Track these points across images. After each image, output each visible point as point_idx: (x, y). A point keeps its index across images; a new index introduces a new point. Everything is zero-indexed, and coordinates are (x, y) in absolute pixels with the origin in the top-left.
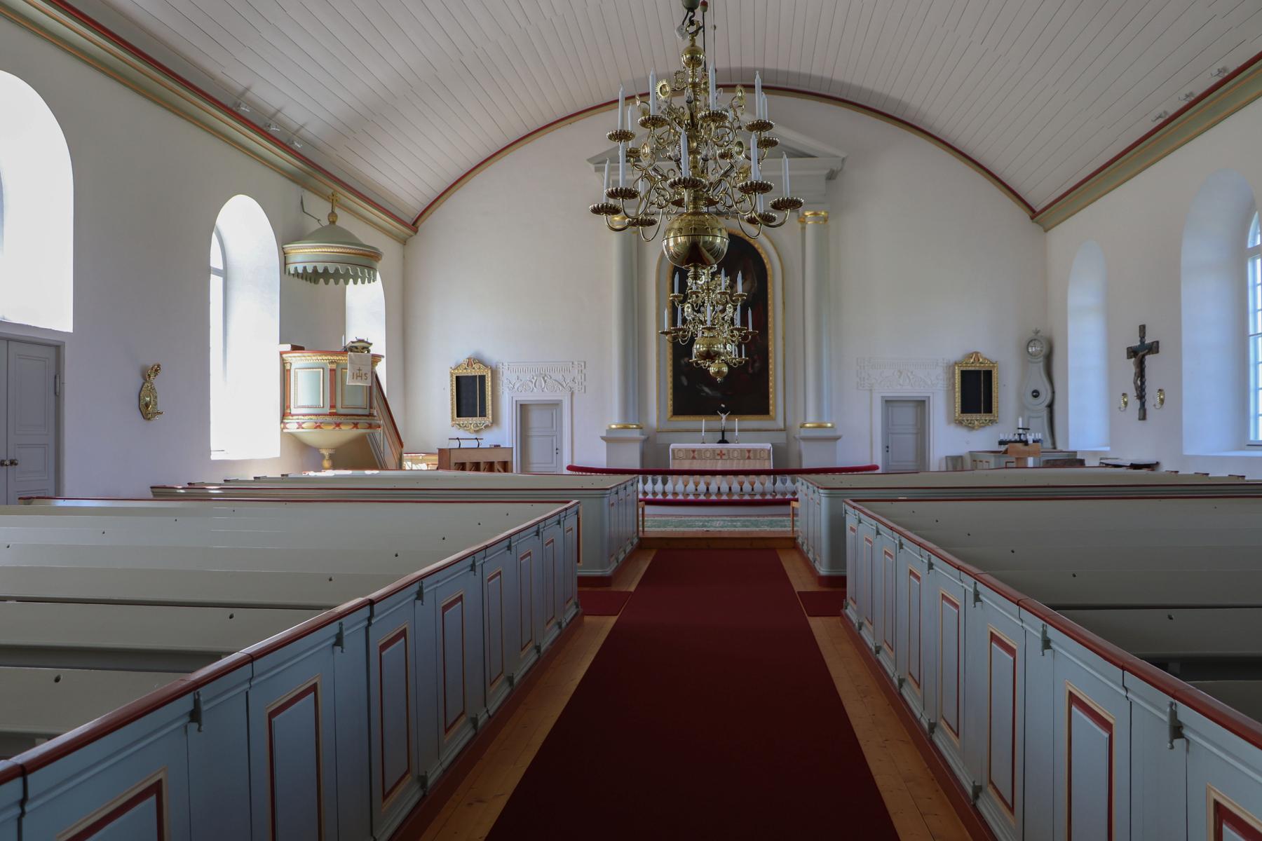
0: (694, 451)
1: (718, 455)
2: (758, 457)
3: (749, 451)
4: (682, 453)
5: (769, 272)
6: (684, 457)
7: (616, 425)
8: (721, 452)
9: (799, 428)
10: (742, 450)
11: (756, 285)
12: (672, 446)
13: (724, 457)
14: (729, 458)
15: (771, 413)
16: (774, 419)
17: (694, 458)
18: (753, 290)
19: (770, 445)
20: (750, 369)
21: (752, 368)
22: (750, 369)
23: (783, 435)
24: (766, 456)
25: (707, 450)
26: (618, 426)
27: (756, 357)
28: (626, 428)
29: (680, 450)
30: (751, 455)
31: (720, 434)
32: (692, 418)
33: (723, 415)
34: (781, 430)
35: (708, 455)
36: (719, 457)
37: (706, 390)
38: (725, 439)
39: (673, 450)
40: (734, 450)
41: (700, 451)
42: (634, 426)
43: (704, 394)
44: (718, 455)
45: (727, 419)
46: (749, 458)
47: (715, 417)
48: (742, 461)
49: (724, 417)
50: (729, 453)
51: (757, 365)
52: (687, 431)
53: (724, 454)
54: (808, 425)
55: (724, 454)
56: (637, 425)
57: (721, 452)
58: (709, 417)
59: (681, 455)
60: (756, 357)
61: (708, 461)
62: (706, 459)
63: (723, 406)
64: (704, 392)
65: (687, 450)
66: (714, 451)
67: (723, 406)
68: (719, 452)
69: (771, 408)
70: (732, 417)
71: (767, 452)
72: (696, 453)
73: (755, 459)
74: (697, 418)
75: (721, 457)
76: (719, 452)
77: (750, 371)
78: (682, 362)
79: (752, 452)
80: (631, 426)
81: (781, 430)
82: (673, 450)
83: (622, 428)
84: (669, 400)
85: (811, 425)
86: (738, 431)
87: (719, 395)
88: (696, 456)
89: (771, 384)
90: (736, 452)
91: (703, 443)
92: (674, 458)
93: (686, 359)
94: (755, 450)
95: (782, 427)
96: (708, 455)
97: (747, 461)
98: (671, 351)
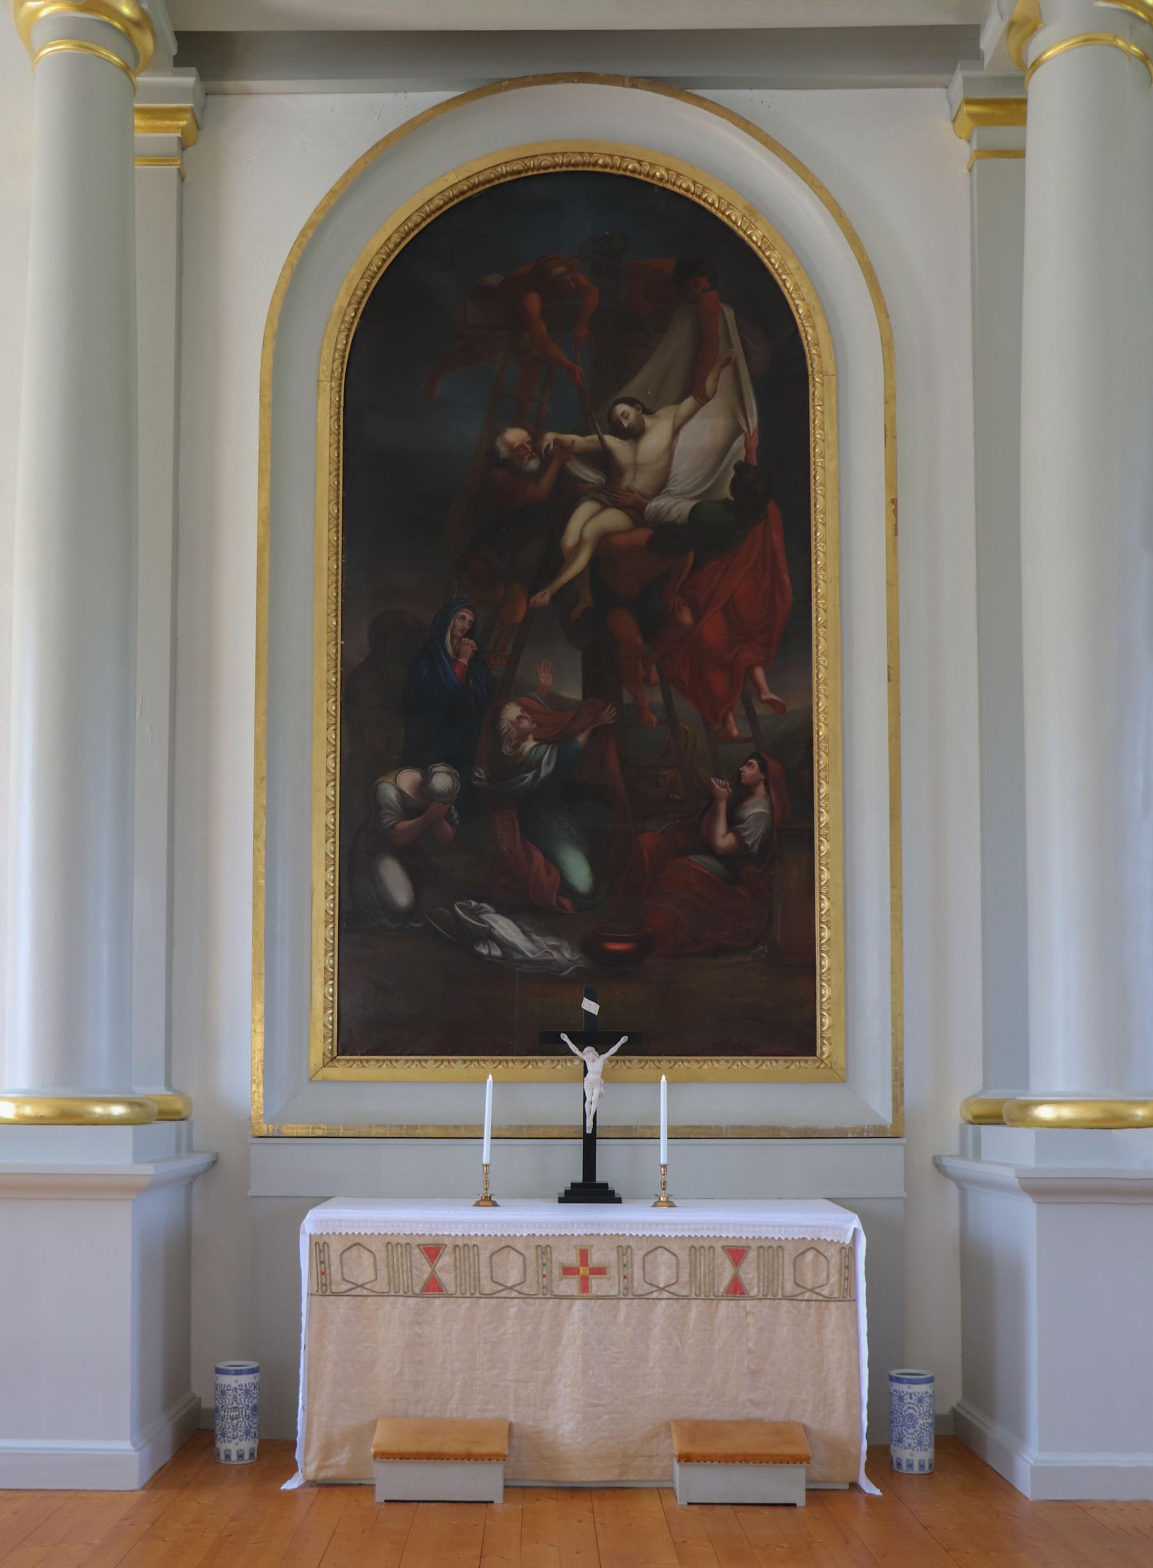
0: (432, 1252)
1: (568, 1271)
2: (789, 1287)
3: (737, 1254)
4: (367, 1259)
5: (819, 359)
6: (382, 1286)
7: (19, 1101)
8: (584, 1255)
9: (955, 1115)
10: (697, 1248)
11: (754, 421)
12: (313, 1223)
13: (597, 1285)
14: (628, 1293)
15: (825, 1049)
16: (839, 1076)
17: (433, 1287)
18: (740, 441)
19: (855, 1223)
20: (721, 826)
21: (733, 823)
22: (721, 826)
23: (888, 1154)
24: (832, 1287)
25: (505, 1246)
26: (28, 1110)
27: (750, 771)
28: (68, 1118)
29: (356, 1244)
30: (749, 1273)
31: (576, 1148)
32: (431, 1068)
33: (589, 1054)
34: (878, 1133)
35: (513, 1276)
36: (570, 1286)
37: (505, 928)
38: (600, 1178)
39: (320, 1246)
40: (657, 1245)
41: (466, 1248)
42: (118, 1110)
43: (497, 952)
44: (568, 1271)
45: (607, 1077)
46: (736, 1289)
47: (545, 1065)
48: (696, 1309)
49: (595, 1061)
50: (625, 1263)
51: (756, 808)
52: (409, 1134)
53: (600, 1271)
54: (1045, 1113)
55: (600, 1271)
56: (130, 1103)
57: (584, 1255)
58: (516, 1066)
59: (363, 1269)
60: (750, 771)
61: (514, 1308)
62: (502, 1292)
63: (590, 1006)
64: (490, 936)
65: (395, 1246)
66: (543, 1249)
67: (590, 1006)
68: (573, 1259)
69: (825, 1022)
70: (634, 1064)
71: (833, 1254)
72: (445, 1260)
73: (770, 1294)
74: (458, 1067)
75: (585, 1287)
76: (573, 1259)
77: (724, 839)
78: (388, 791)
79: (752, 1255)
80: (98, 1110)
81: (878, 1133)
82: (320, 1246)
83: (38, 1121)
84: (319, 979)
85: (1066, 1112)
86: (675, 1135)
87: (565, 954)
88: (447, 1278)
89: (824, 905)
90: (663, 1257)
91: (488, 1201)
92: (323, 1288)
93: (408, 779)
94: (771, 1250)
95: (884, 1114)
96: (514, 1277)
97: (726, 1308)
98: (333, 735)
